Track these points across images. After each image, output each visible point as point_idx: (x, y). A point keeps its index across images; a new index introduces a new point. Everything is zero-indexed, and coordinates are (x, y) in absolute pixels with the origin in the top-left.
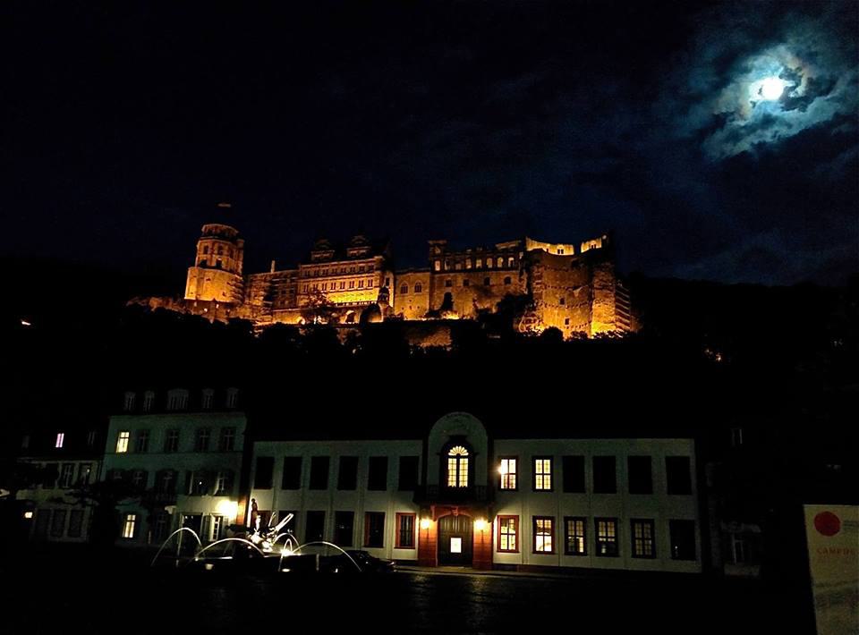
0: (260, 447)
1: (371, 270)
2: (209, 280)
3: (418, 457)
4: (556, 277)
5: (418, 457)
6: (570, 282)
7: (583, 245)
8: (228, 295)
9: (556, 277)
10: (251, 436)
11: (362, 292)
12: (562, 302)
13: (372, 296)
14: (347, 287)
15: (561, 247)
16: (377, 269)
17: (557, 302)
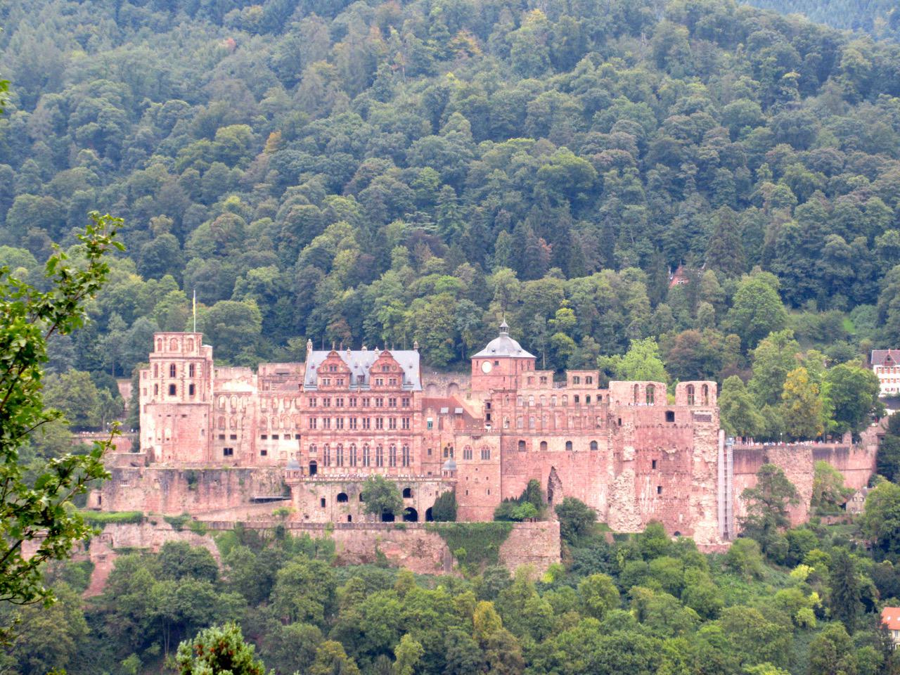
17: (649, 465)
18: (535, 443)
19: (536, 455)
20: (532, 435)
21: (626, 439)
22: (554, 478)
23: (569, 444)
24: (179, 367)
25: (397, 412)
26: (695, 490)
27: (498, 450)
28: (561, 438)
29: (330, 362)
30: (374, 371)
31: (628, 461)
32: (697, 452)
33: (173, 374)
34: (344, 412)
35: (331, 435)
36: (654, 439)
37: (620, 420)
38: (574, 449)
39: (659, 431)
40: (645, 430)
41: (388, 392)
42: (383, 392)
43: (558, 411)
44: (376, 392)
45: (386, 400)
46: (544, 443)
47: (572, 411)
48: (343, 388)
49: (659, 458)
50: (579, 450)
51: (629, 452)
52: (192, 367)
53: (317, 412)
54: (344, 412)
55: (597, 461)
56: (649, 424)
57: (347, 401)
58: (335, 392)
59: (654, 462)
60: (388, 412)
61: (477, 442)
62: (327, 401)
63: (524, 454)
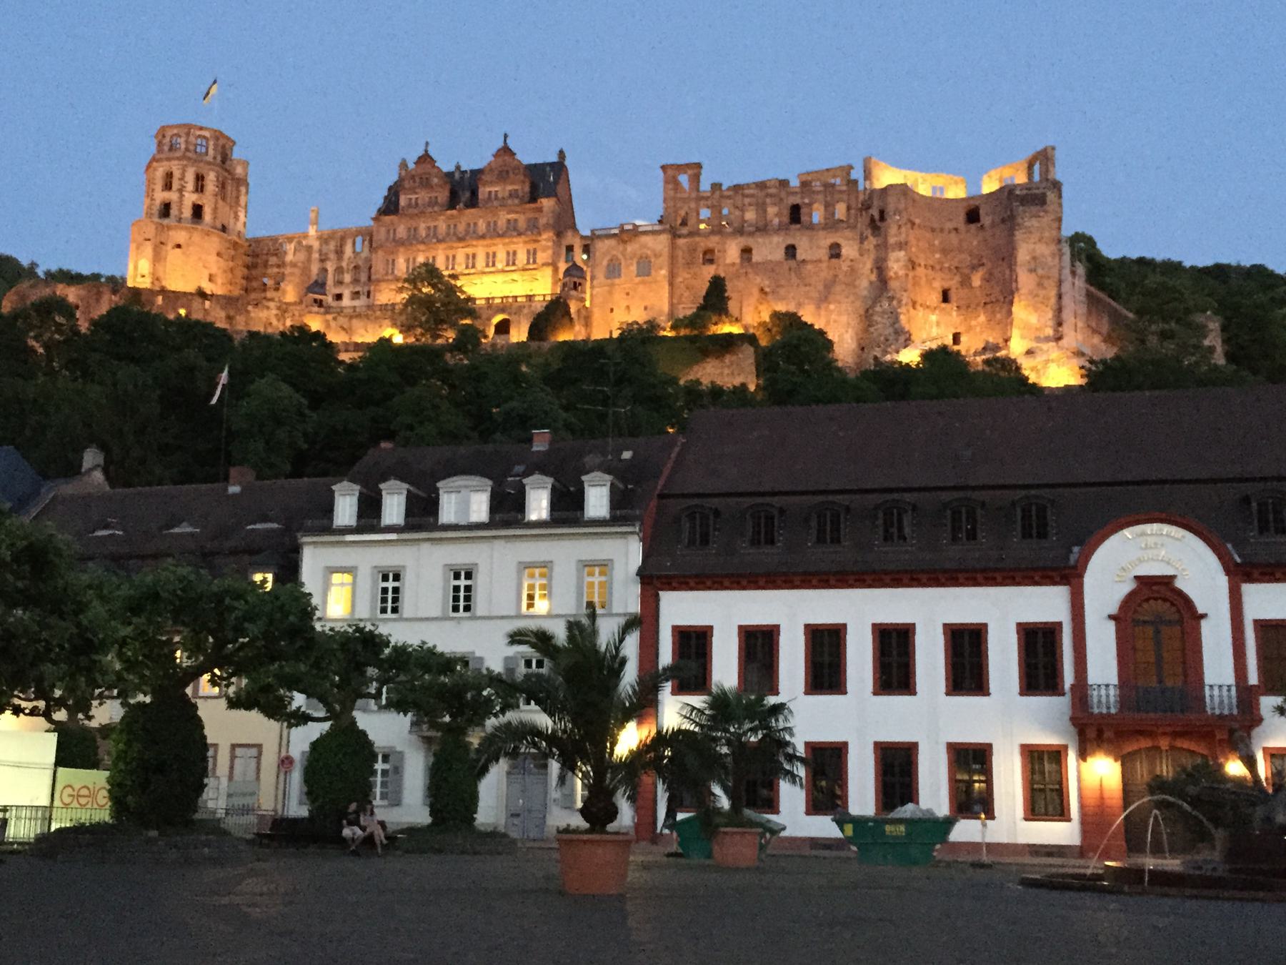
0: (681, 608)
1: (534, 228)
2: (179, 246)
3: (1060, 624)
4: (931, 245)
5: (1060, 624)
6: (963, 256)
7: (985, 178)
8: (219, 281)
9: (931, 245)
10: (654, 580)
11: (515, 276)
12: (946, 297)
13: (542, 286)
14: (480, 262)
15: (939, 180)
16: (547, 227)
17: (935, 298)
19: (731, 269)
21: (892, 240)
23: (791, 251)
24: (177, 174)
28: (776, 239)
29: (420, 171)
32: (1023, 255)
33: (168, 186)
36: (945, 251)
37: (882, 213)
39: (954, 239)
40: (928, 235)
43: (771, 196)
46: (747, 251)
47: (795, 193)
49: (953, 283)
50: (808, 258)
51: (896, 263)
52: (200, 179)
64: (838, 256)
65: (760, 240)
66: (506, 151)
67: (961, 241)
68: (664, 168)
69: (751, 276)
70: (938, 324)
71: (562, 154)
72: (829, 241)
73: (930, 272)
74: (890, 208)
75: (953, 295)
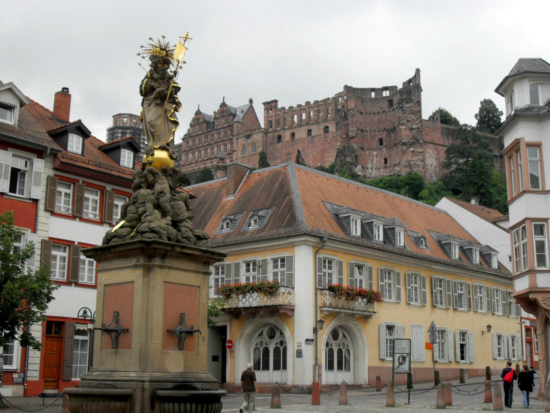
12: (381, 144)
17: (376, 143)
18: (287, 135)
20: (284, 129)
22: (300, 159)
23: (309, 131)
25: (227, 140)
26: (404, 153)
27: (260, 144)
28: (303, 128)
30: (217, 117)
31: (353, 138)
34: (201, 147)
35: (195, 163)
38: (313, 135)
39: (384, 116)
41: (223, 128)
42: (220, 129)
44: (217, 130)
45: (222, 134)
46: (293, 135)
48: (201, 132)
49: (383, 135)
53: (189, 150)
54: (201, 147)
55: (329, 141)
56: (376, 112)
57: (203, 139)
58: (197, 135)
59: (381, 142)
60: (223, 141)
61: (249, 140)
62: (194, 141)
63: (281, 143)
64: (328, 132)
65: (298, 129)
66: (223, 105)
67: (387, 116)
68: (264, 104)
69: (294, 145)
70: (377, 156)
71: (251, 101)
72: (324, 126)
73: (372, 132)
74: (349, 109)
75: (384, 143)
